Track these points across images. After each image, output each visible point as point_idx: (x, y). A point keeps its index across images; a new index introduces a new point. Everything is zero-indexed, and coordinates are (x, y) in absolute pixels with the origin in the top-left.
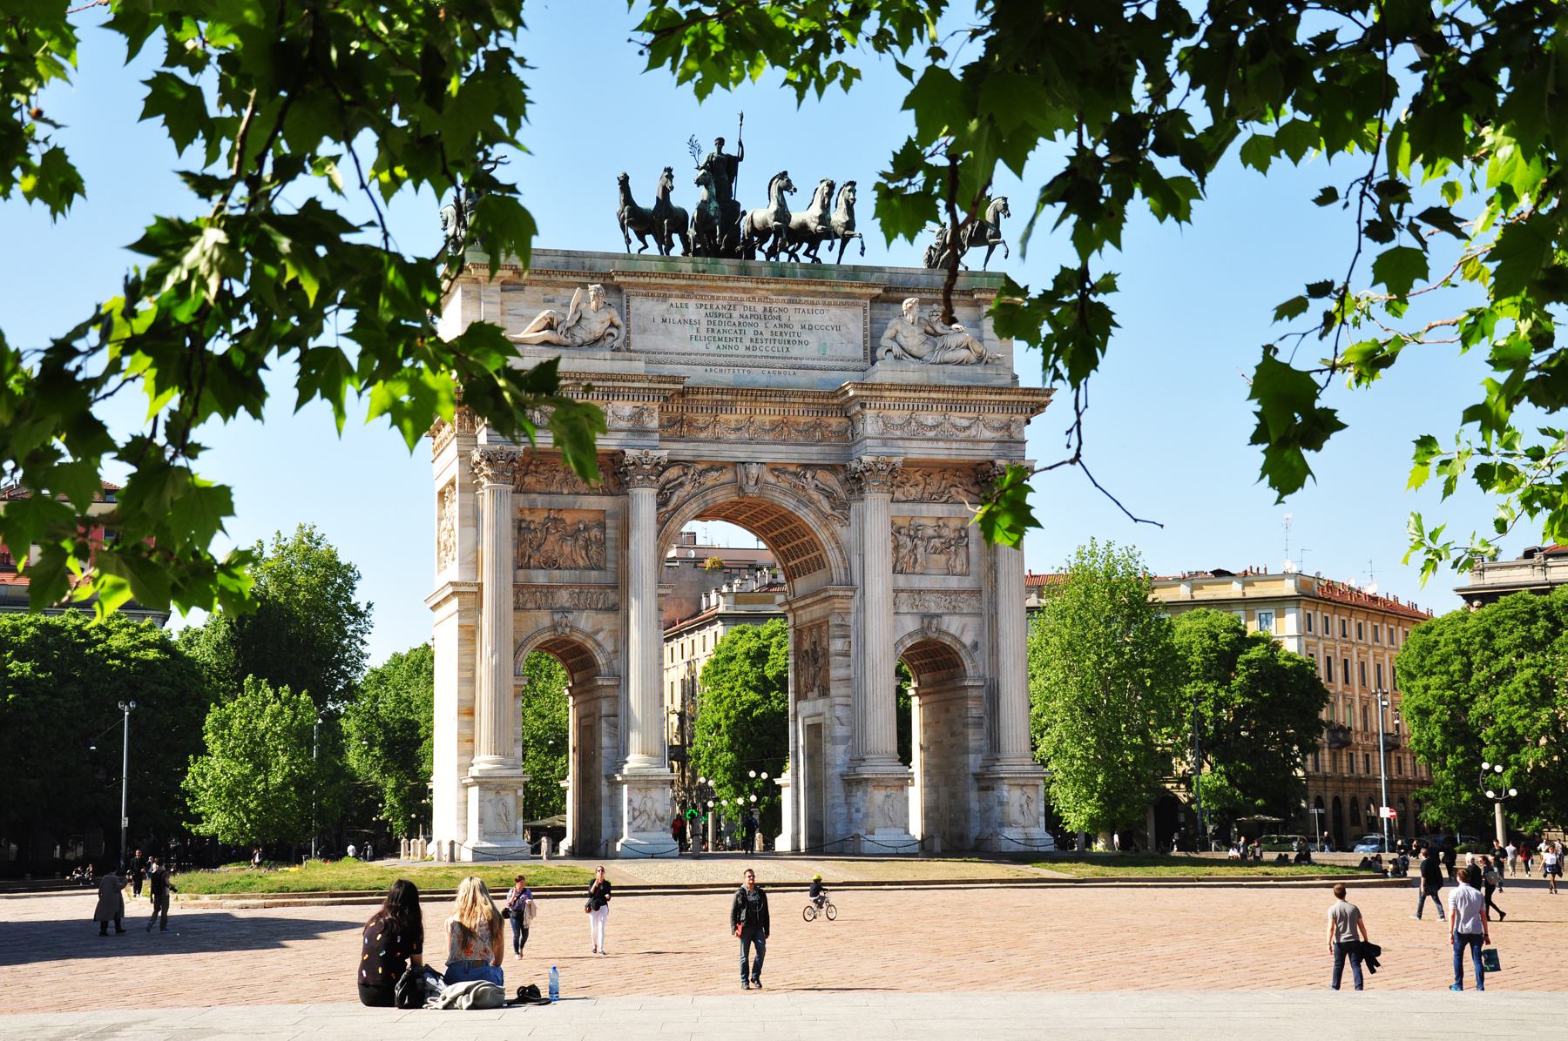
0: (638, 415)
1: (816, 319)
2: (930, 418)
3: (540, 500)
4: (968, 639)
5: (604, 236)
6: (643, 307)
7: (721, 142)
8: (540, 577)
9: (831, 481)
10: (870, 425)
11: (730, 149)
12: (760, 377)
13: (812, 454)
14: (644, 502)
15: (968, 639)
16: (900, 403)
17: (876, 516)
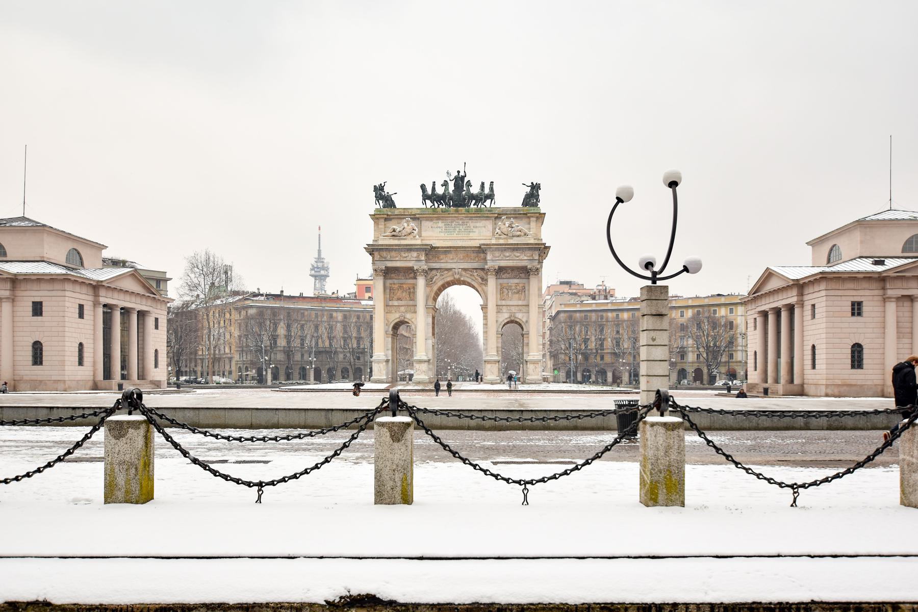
0: (418, 257)
1: (478, 224)
2: (507, 254)
3: (396, 281)
4: (524, 320)
6: (426, 224)
7: (459, 172)
8: (396, 303)
9: (482, 273)
10: (489, 257)
11: (462, 174)
13: (476, 265)
14: (421, 282)
15: (524, 320)
16: (498, 249)
17: (492, 282)
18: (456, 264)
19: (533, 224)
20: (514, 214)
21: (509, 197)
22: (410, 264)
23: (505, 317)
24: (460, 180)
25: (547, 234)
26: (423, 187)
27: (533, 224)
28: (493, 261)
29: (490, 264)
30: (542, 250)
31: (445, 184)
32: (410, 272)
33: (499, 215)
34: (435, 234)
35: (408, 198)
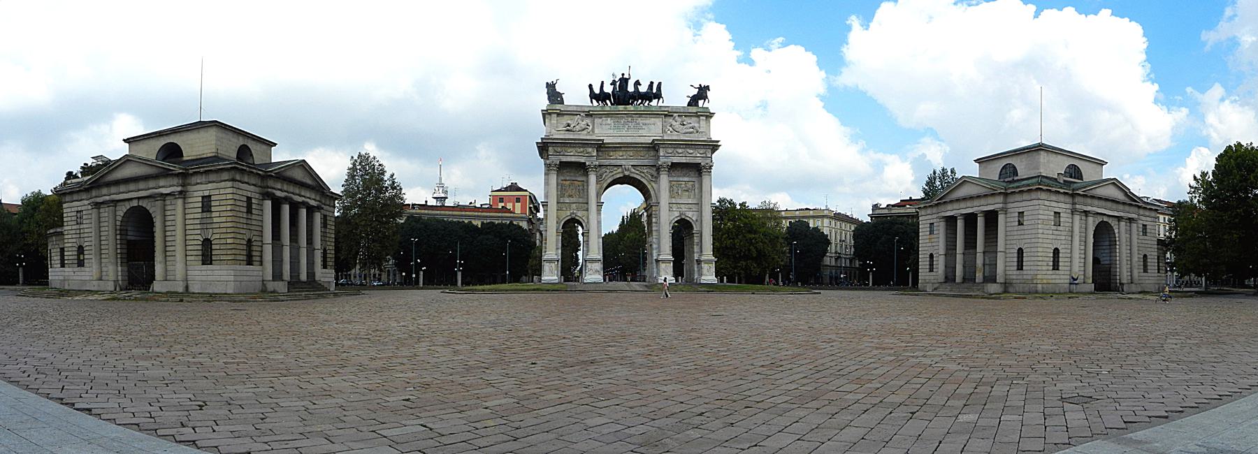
5: (584, 100)
6: (597, 121)
12: (629, 140)
13: (646, 162)
14: (592, 178)
17: (664, 179)
18: (627, 162)
19: (703, 123)
20: (682, 113)
21: (675, 97)
22: (582, 160)
23: (675, 215)
24: (624, 81)
25: (716, 130)
26: (590, 86)
27: (703, 123)
28: (666, 157)
29: (662, 160)
30: (714, 146)
31: (614, 83)
32: (582, 168)
33: (668, 114)
34: (606, 131)
35: (576, 97)
